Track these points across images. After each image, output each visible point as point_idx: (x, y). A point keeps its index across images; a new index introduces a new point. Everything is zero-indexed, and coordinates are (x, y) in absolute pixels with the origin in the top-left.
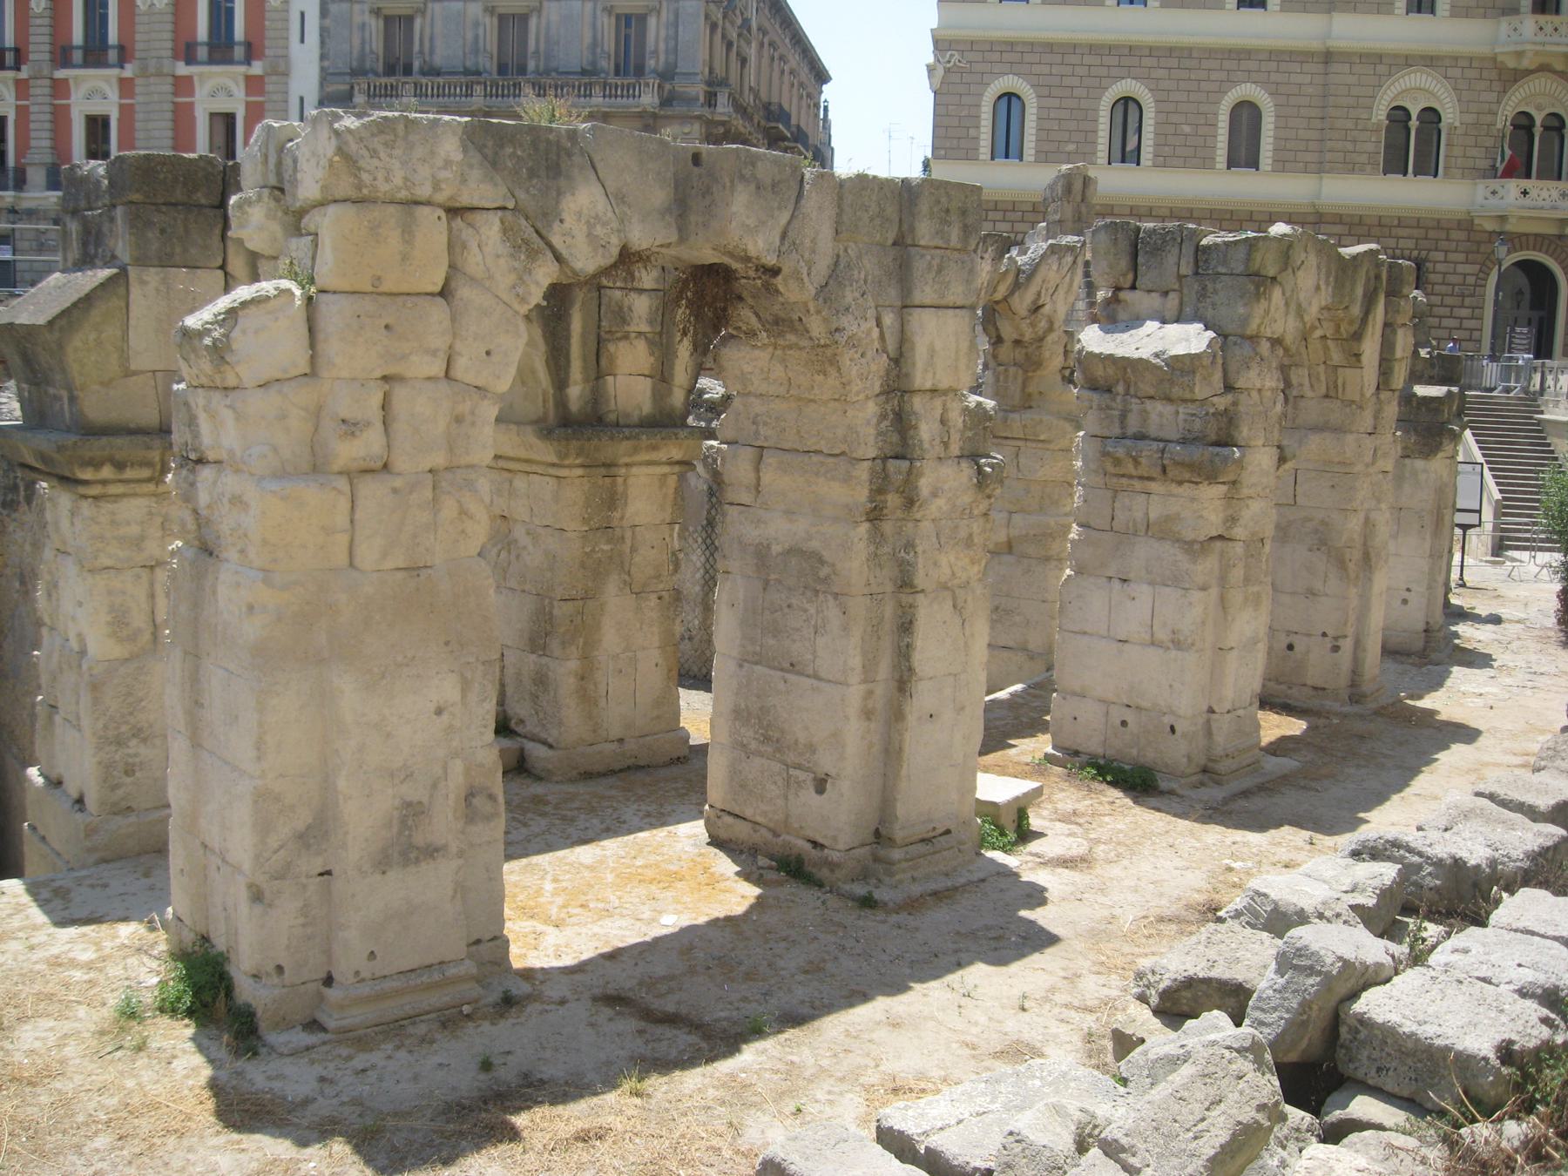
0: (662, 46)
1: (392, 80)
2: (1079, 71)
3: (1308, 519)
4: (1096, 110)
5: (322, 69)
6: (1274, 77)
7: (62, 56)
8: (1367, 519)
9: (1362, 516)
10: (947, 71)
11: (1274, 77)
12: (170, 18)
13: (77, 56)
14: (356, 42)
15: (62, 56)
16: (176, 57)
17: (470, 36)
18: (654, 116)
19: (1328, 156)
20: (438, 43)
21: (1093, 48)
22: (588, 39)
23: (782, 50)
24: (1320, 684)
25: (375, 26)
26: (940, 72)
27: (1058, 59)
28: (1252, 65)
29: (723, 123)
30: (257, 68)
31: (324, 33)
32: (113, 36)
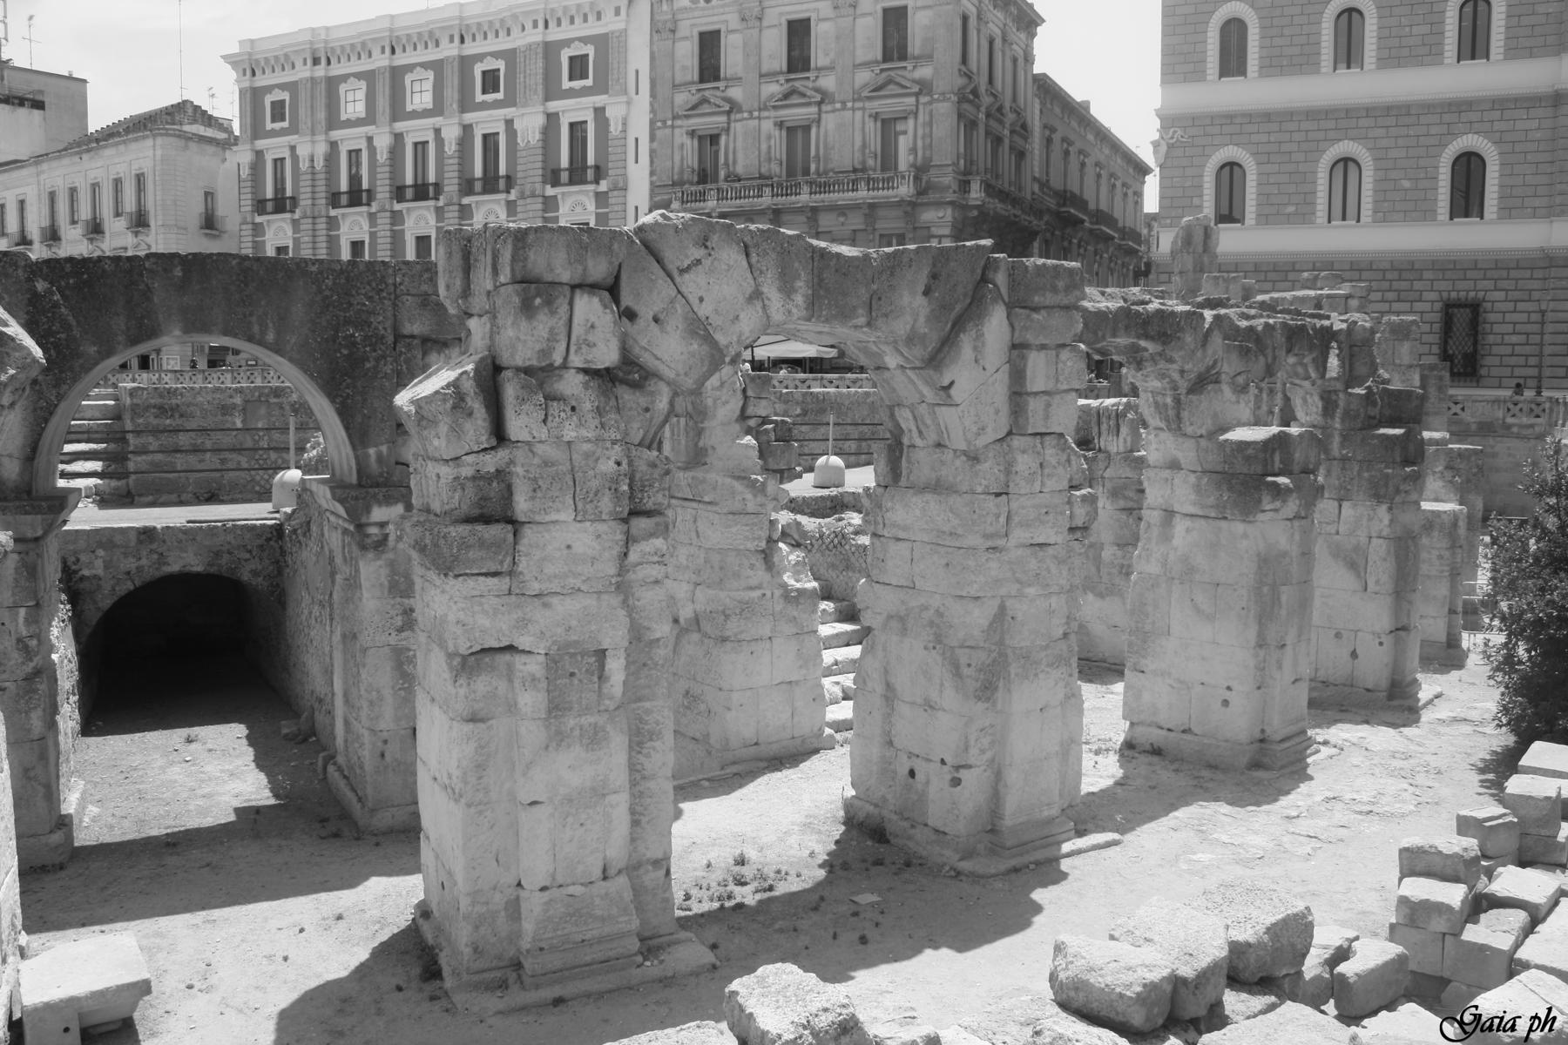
0: (920, 143)
1: (700, 187)
2: (1296, 137)
3: (926, 608)
4: (1315, 173)
5: (652, 183)
6: (1498, 126)
7: (467, 187)
8: (1002, 608)
9: (991, 607)
10: (1170, 147)
11: (1498, 126)
12: (540, 151)
13: (478, 186)
14: (677, 158)
15: (467, 187)
16: (544, 182)
17: (764, 147)
18: (913, 205)
19: (1558, 200)
20: (740, 156)
21: (1312, 114)
22: (858, 143)
23: (1079, 144)
24: (939, 825)
25: (691, 145)
26: (1164, 148)
27: (1275, 127)
28: (1473, 116)
29: (977, 207)
30: (603, 186)
31: (652, 152)
32: (502, 171)
